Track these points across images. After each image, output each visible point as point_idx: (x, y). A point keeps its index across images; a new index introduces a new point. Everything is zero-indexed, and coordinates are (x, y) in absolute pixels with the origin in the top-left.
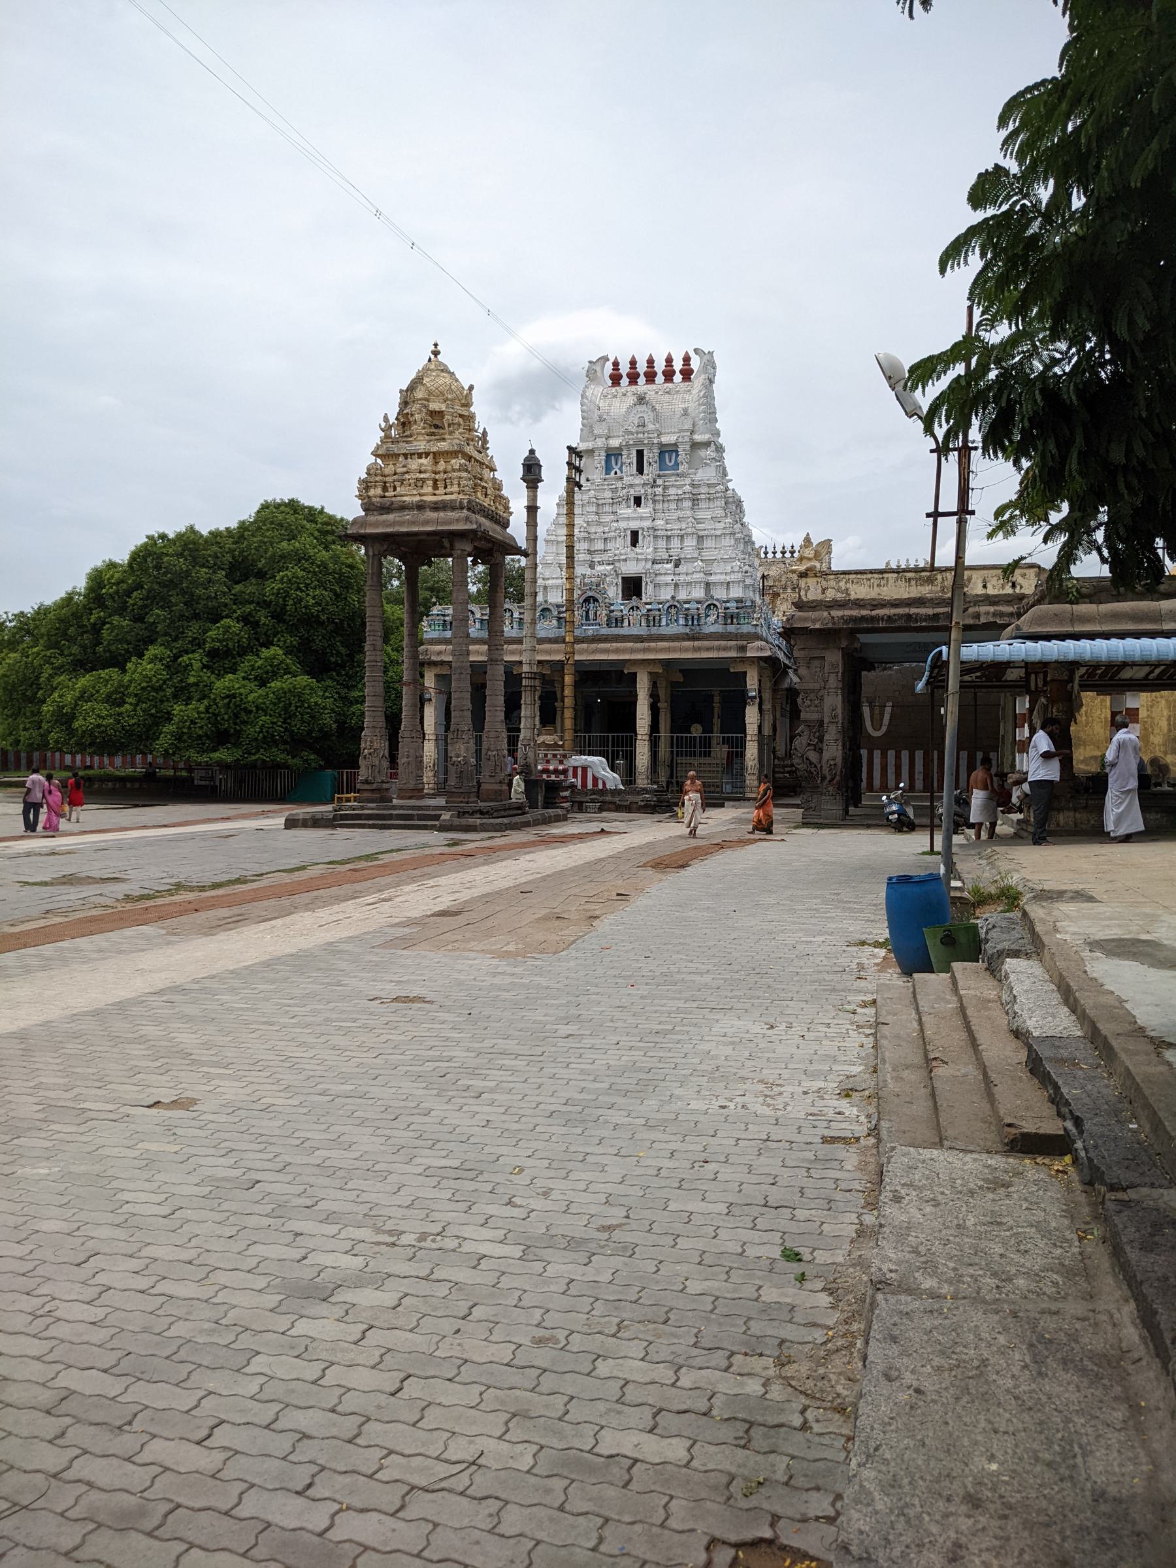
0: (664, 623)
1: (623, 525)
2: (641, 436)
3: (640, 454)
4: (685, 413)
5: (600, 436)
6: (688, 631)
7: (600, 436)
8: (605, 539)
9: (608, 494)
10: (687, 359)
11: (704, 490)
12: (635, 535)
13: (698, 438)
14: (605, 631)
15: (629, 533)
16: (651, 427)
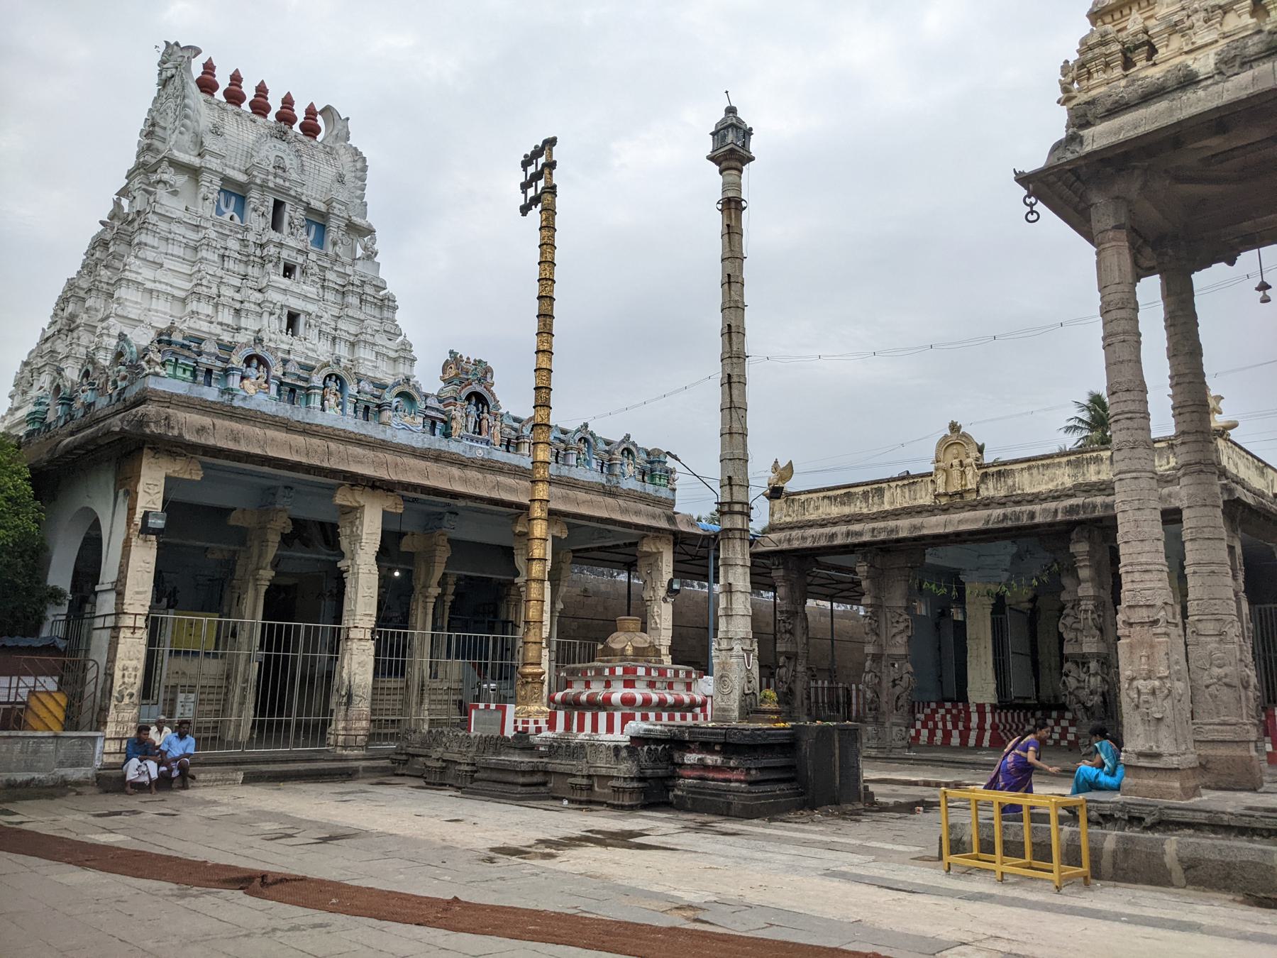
0: (572, 460)
1: (274, 296)
2: (281, 182)
3: (278, 205)
4: (341, 179)
5: (213, 154)
6: (604, 481)
7: (213, 154)
8: (237, 311)
9: (233, 244)
10: (311, 112)
11: (369, 290)
12: (293, 319)
13: (357, 220)
14: (500, 455)
15: (286, 311)
16: (294, 176)
